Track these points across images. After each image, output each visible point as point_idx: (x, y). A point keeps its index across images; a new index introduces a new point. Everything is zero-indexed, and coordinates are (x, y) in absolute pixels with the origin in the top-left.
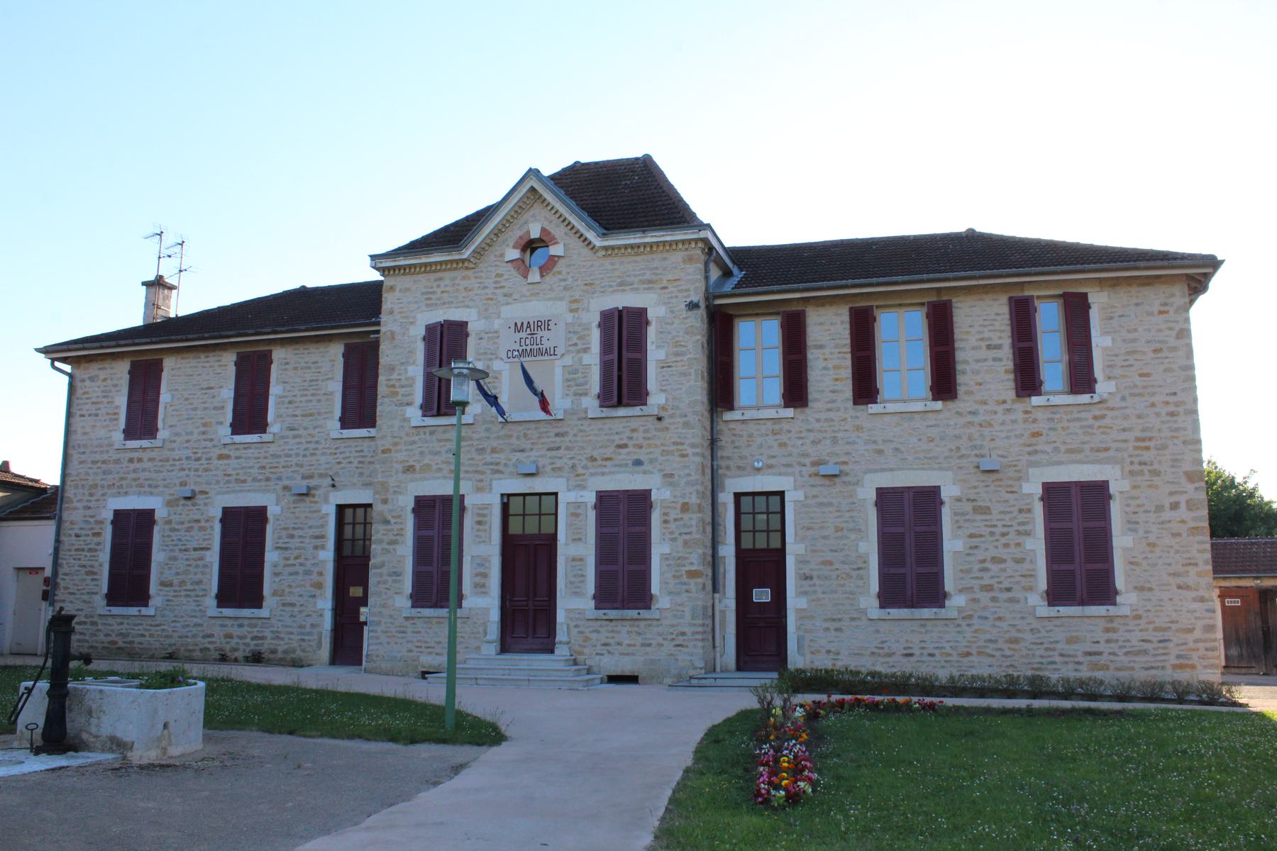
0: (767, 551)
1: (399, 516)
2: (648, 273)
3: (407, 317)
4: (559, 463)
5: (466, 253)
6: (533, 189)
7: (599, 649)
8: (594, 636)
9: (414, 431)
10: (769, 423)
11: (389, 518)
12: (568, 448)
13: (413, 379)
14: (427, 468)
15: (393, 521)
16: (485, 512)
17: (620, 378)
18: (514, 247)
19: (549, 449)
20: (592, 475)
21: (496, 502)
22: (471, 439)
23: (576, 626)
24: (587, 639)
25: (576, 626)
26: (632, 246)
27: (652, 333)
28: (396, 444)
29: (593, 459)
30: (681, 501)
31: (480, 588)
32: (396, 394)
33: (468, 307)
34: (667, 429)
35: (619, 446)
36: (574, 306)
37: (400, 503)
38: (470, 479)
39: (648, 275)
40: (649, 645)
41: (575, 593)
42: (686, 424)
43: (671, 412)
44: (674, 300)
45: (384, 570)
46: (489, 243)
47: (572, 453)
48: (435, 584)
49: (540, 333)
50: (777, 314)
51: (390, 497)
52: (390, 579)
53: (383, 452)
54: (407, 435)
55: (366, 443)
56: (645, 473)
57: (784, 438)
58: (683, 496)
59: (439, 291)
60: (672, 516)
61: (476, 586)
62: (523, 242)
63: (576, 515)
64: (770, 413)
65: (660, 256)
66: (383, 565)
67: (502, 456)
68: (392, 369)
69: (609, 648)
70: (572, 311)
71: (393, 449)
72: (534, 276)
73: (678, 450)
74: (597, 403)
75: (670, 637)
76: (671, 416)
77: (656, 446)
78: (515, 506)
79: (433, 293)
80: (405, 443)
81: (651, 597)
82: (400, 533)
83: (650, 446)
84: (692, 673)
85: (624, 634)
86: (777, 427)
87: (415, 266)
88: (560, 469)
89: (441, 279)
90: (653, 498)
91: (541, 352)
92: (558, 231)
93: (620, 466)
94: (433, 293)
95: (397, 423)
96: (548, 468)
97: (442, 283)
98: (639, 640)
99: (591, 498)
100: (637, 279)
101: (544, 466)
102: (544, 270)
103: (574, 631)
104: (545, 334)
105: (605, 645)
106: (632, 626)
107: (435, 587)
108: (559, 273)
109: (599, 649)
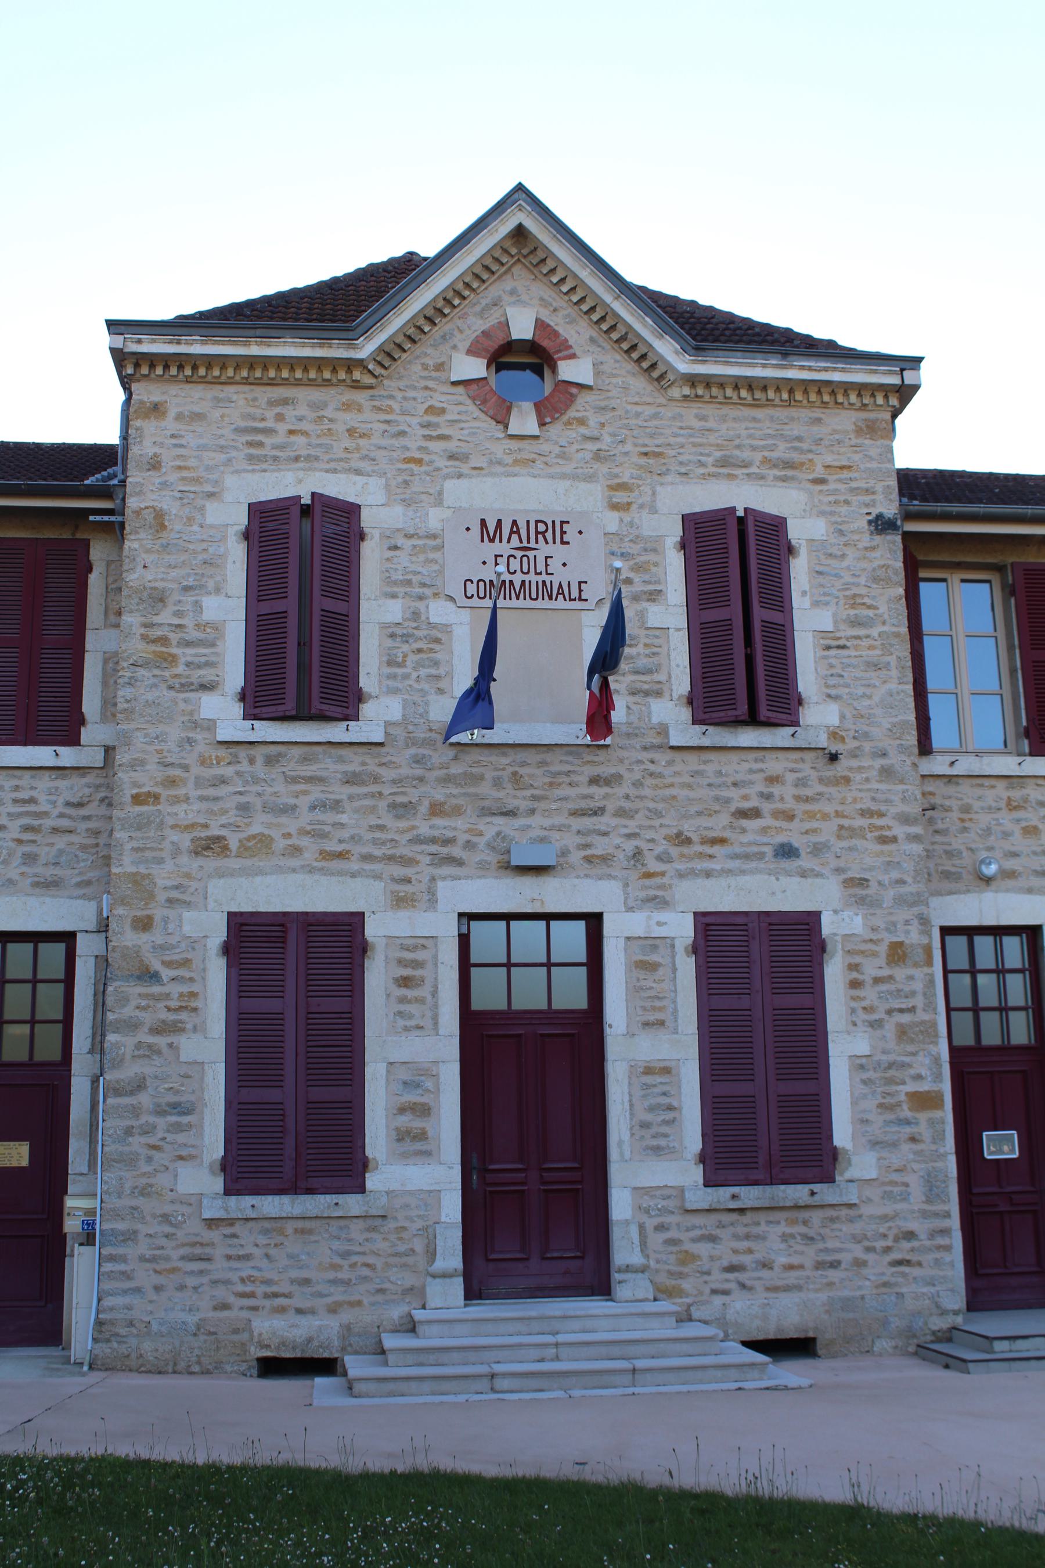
0: (1006, 1049)
1: (186, 963)
2: (782, 446)
3: (197, 480)
4: (601, 846)
5: (366, 348)
6: (520, 233)
7: (718, 1279)
8: (703, 1249)
9: (222, 752)
10: (1001, 785)
11: (156, 965)
12: (621, 813)
13: (218, 628)
14: (262, 844)
15: (166, 974)
16: (420, 955)
17: (750, 660)
18: (470, 352)
19: (574, 813)
20: (681, 875)
21: (446, 930)
22: (376, 779)
23: (660, 1228)
24: (688, 1258)
25: (660, 1228)
26: (751, 384)
27: (800, 572)
28: (172, 782)
29: (681, 840)
30: (889, 938)
31: (413, 1141)
32: (173, 659)
33: (358, 472)
34: (847, 780)
35: (742, 814)
36: (621, 497)
37: (187, 929)
38: (378, 877)
39: (782, 451)
40: (835, 1265)
41: (657, 1150)
42: (887, 773)
43: (851, 744)
44: (844, 509)
45: (144, 1099)
46: (411, 337)
47: (632, 825)
48: (295, 1126)
49: (544, 549)
50: (1000, 569)
51: (158, 913)
52: (161, 1122)
53: (137, 799)
54: (203, 762)
55: (45, 782)
56: (803, 874)
57: (1030, 816)
58: (891, 928)
59: (282, 428)
60: (871, 969)
61: (402, 1136)
62: (494, 345)
63: (651, 967)
64: (1008, 765)
65: (804, 414)
66: (139, 1085)
67: (460, 823)
68: (159, 599)
69: (741, 1276)
70: (615, 507)
71: (165, 793)
72: (524, 420)
73: (873, 828)
74: (686, 714)
75: (880, 1244)
76: (854, 754)
77: (825, 817)
78: (488, 940)
79: (268, 431)
80: (199, 782)
81: (834, 1154)
82: (189, 1004)
83: (811, 815)
84: (940, 1324)
85: (774, 1240)
86: (1016, 794)
87: (223, 361)
88: (605, 859)
89: (285, 402)
90: (826, 930)
91: (547, 591)
92: (575, 331)
93: (747, 857)
94: (268, 431)
95: (175, 733)
96: (576, 857)
97: (289, 412)
98: (809, 1255)
99: (682, 929)
100: (758, 457)
101: (564, 853)
102: (548, 411)
103: (656, 1240)
104: (557, 551)
105: (731, 1268)
106: (793, 1222)
107: (290, 1143)
108: (582, 422)
109: (718, 1279)
